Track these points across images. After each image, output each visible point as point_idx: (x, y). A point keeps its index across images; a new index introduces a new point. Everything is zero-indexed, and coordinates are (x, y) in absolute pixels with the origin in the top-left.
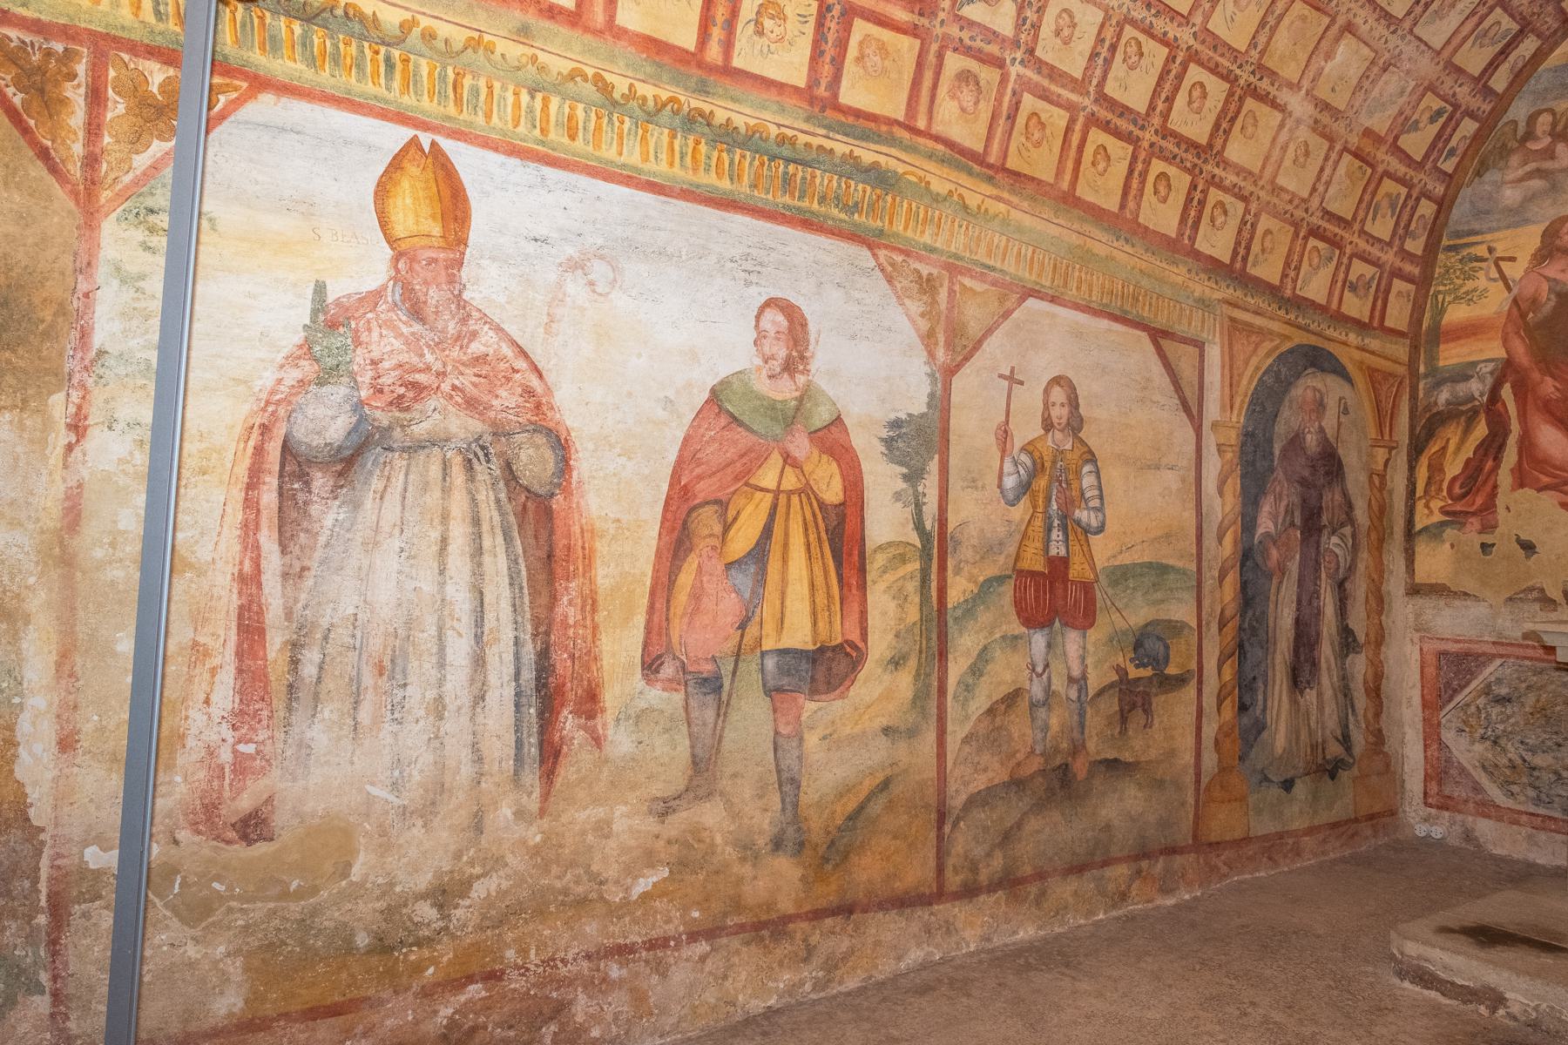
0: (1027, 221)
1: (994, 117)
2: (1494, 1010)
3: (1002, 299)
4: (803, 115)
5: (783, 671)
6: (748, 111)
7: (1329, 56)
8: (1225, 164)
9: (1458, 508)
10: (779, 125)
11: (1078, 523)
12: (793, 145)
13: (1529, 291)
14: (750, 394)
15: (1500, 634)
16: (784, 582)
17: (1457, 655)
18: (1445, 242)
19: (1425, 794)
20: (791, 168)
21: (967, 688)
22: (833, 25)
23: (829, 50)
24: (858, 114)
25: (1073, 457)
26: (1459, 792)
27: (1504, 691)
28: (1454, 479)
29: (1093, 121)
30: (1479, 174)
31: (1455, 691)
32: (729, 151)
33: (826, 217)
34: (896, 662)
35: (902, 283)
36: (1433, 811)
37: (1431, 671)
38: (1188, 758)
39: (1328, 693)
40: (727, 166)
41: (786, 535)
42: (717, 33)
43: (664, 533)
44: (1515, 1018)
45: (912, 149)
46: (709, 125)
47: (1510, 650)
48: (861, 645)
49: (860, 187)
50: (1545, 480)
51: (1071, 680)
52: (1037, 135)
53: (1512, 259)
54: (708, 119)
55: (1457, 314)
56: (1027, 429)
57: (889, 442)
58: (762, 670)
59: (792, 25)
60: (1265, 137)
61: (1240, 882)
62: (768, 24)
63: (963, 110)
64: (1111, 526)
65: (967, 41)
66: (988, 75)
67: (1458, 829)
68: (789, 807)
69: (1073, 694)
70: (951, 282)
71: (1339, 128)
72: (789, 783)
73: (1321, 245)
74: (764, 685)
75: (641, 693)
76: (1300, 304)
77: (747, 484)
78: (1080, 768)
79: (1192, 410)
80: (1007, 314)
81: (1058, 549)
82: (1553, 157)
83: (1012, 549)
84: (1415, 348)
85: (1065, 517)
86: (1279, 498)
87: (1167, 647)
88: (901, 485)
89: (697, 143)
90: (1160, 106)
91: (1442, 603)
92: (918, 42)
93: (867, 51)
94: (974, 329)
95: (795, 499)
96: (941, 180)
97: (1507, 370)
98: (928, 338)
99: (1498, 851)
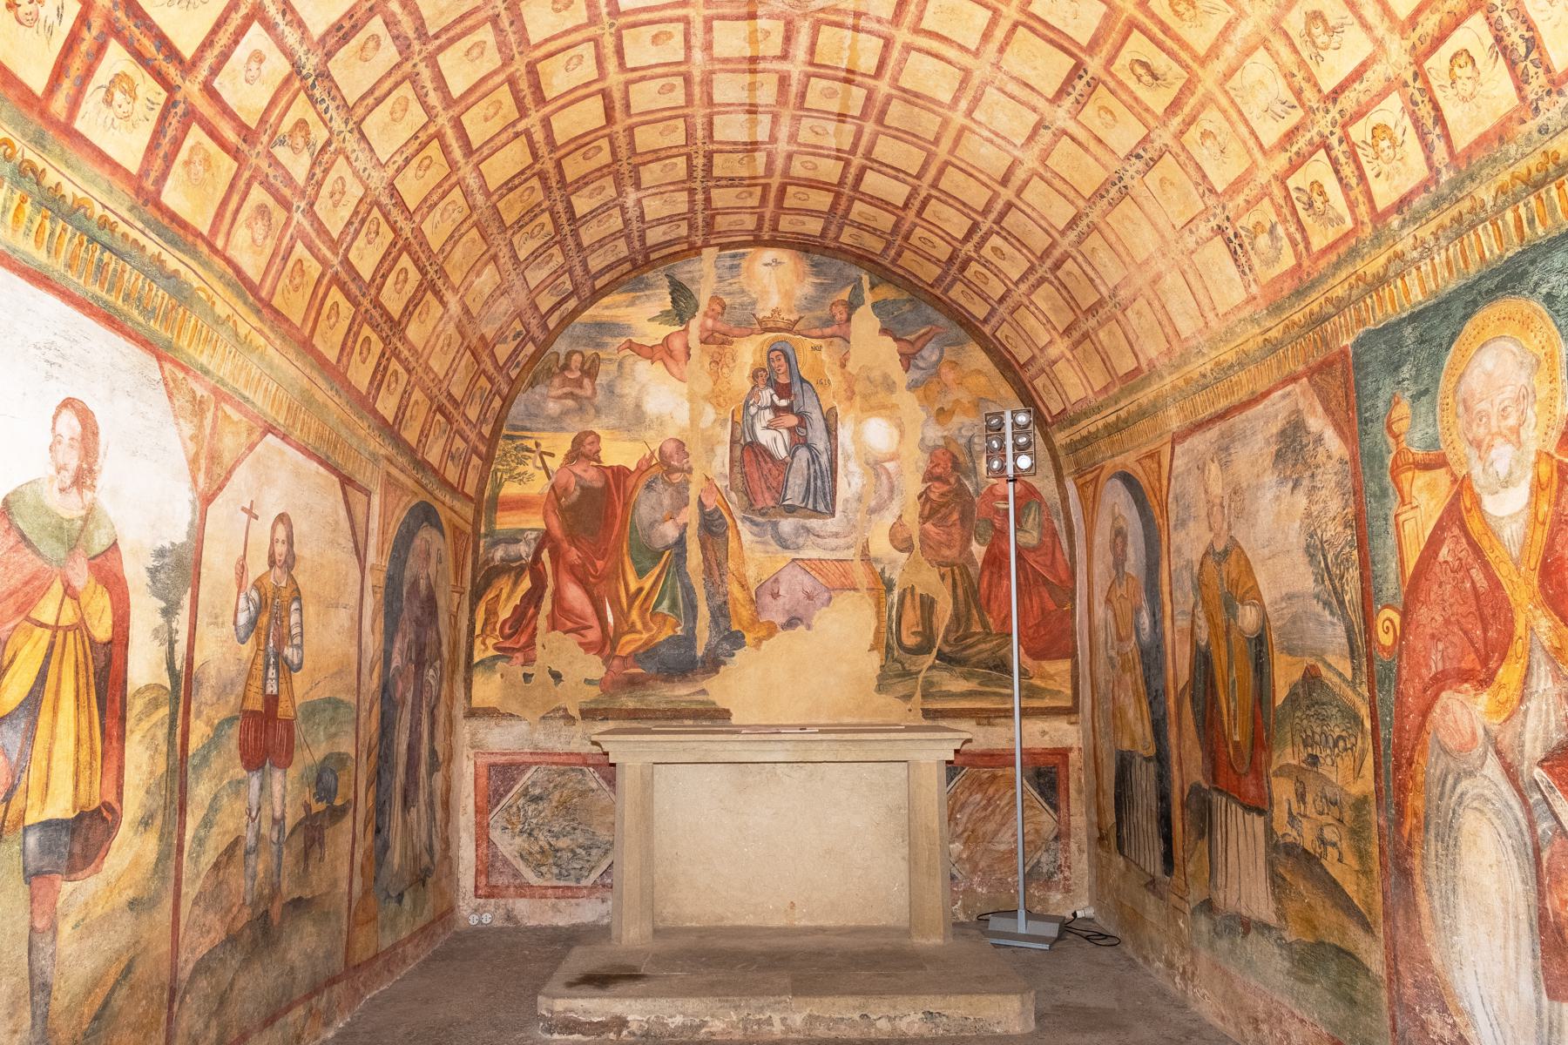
0: (277, 359)
1: (274, 255)
2: (619, 1033)
3: (250, 431)
4: (128, 204)
5: (46, 849)
6: (78, 181)
7: (478, 275)
8: (403, 339)
9: (507, 644)
10: (105, 207)
11: (286, 659)
12: (113, 231)
13: (563, 481)
14: (41, 508)
15: (536, 747)
16: (53, 737)
17: (503, 765)
18: (505, 431)
19: (476, 887)
20: (107, 254)
21: (200, 842)
22: (174, 122)
23: (165, 142)
24: (173, 217)
25: (286, 594)
26: (500, 880)
27: (538, 791)
28: (505, 622)
29: (336, 279)
30: (532, 385)
31: (502, 796)
32: (52, 220)
33: (128, 317)
34: (145, 822)
35: (181, 401)
36: (482, 901)
37: (483, 781)
38: (344, 886)
39: (423, 808)
41: (59, 679)
42: (67, 86)
44: (634, 1034)
45: (206, 265)
46: (38, 183)
47: (543, 758)
48: (116, 806)
49: (161, 292)
50: (570, 625)
51: (275, 821)
52: (297, 280)
53: (552, 455)
54: (38, 175)
55: (510, 489)
56: (258, 567)
57: (153, 572)
58: (23, 851)
59: (140, 107)
60: (430, 324)
61: (373, 999)
62: (118, 96)
63: (254, 241)
64: (307, 664)
65: (272, 180)
66: (279, 215)
67: (501, 911)
68: (39, 1021)
69: (275, 836)
70: (216, 408)
71: (469, 329)
72: (40, 987)
73: (442, 420)
74: (25, 869)
76: (422, 465)
77: (28, 618)
78: (276, 910)
79: (360, 553)
80: (251, 448)
81: (272, 688)
82: (581, 386)
83: (240, 689)
84: (478, 512)
85: (278, 655)
86: (404, 637)
87: (336, 779)
88: (160, 620)
89: (23, 201)
90: (378, 280)
91: (493, 723)
92: (236, 165)
93: (196, 159)
94: (227, 458)
95: (70, 635)
96: (225, 303)
97: (545, 539)
98: (194, 461)
99: (532, 923)
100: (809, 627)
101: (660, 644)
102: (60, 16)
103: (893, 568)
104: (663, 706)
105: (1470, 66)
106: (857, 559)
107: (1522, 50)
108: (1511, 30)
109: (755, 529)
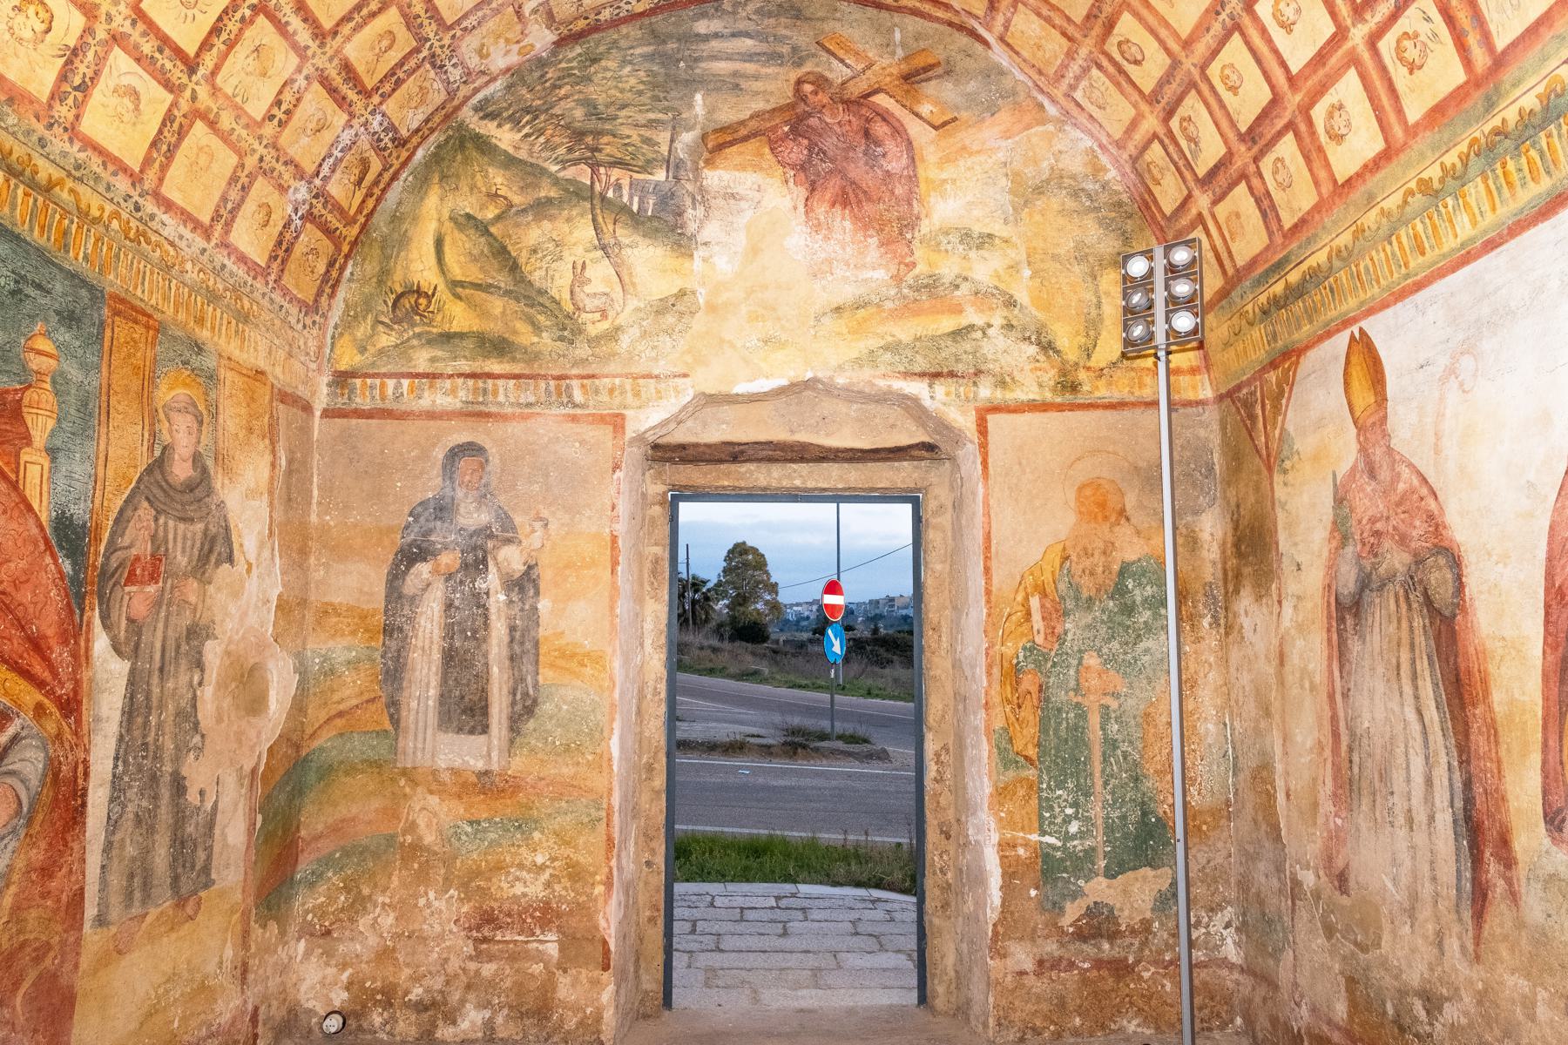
32: (1533, 145)
40: (1539, 163)
43: (1549, 651)
75: (1547, 852)
89: (1504, 165)
102: (1428, 19)
105: (44, 27)
107: (77, 81)
108: (86, 61)
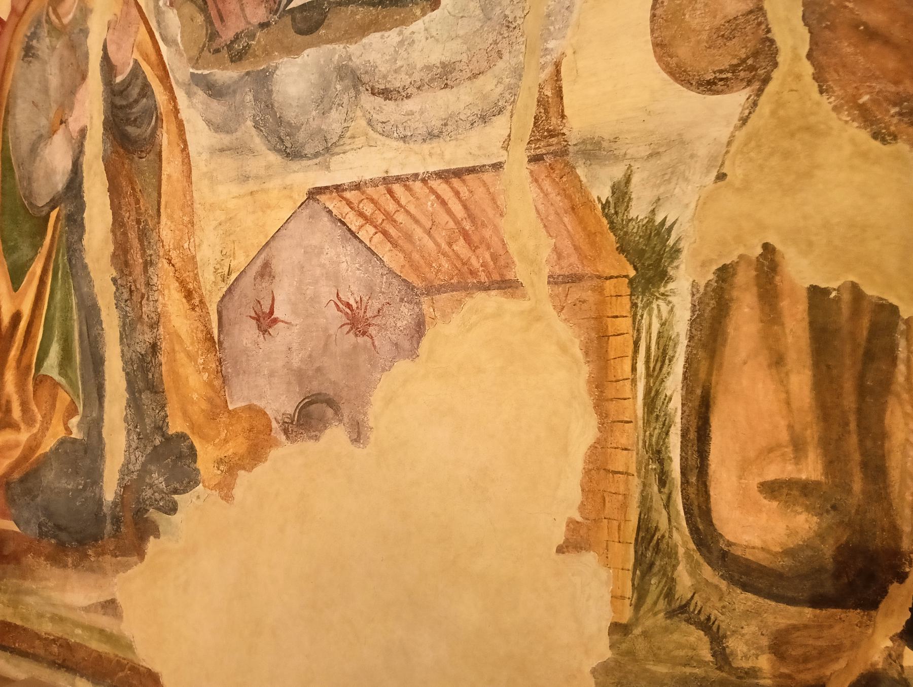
100: (358, 433)
101: (45, 460)
103: (671, 174)
104: (47, 628)
106: (520, 153)
109: (218, 107)
